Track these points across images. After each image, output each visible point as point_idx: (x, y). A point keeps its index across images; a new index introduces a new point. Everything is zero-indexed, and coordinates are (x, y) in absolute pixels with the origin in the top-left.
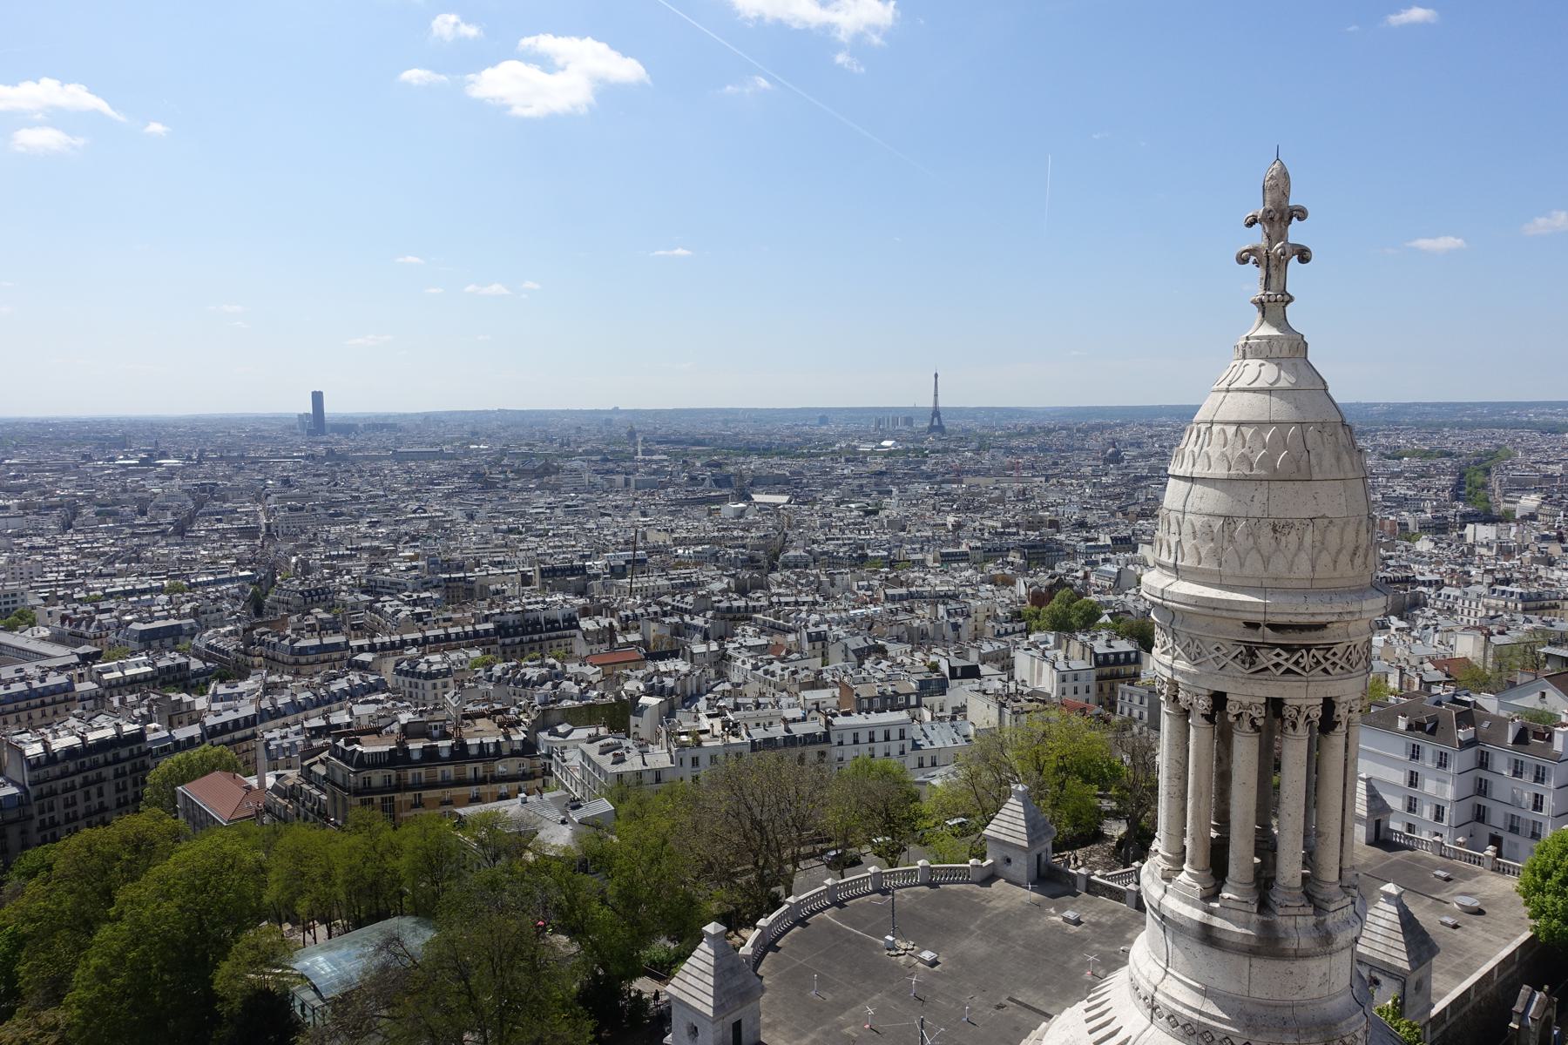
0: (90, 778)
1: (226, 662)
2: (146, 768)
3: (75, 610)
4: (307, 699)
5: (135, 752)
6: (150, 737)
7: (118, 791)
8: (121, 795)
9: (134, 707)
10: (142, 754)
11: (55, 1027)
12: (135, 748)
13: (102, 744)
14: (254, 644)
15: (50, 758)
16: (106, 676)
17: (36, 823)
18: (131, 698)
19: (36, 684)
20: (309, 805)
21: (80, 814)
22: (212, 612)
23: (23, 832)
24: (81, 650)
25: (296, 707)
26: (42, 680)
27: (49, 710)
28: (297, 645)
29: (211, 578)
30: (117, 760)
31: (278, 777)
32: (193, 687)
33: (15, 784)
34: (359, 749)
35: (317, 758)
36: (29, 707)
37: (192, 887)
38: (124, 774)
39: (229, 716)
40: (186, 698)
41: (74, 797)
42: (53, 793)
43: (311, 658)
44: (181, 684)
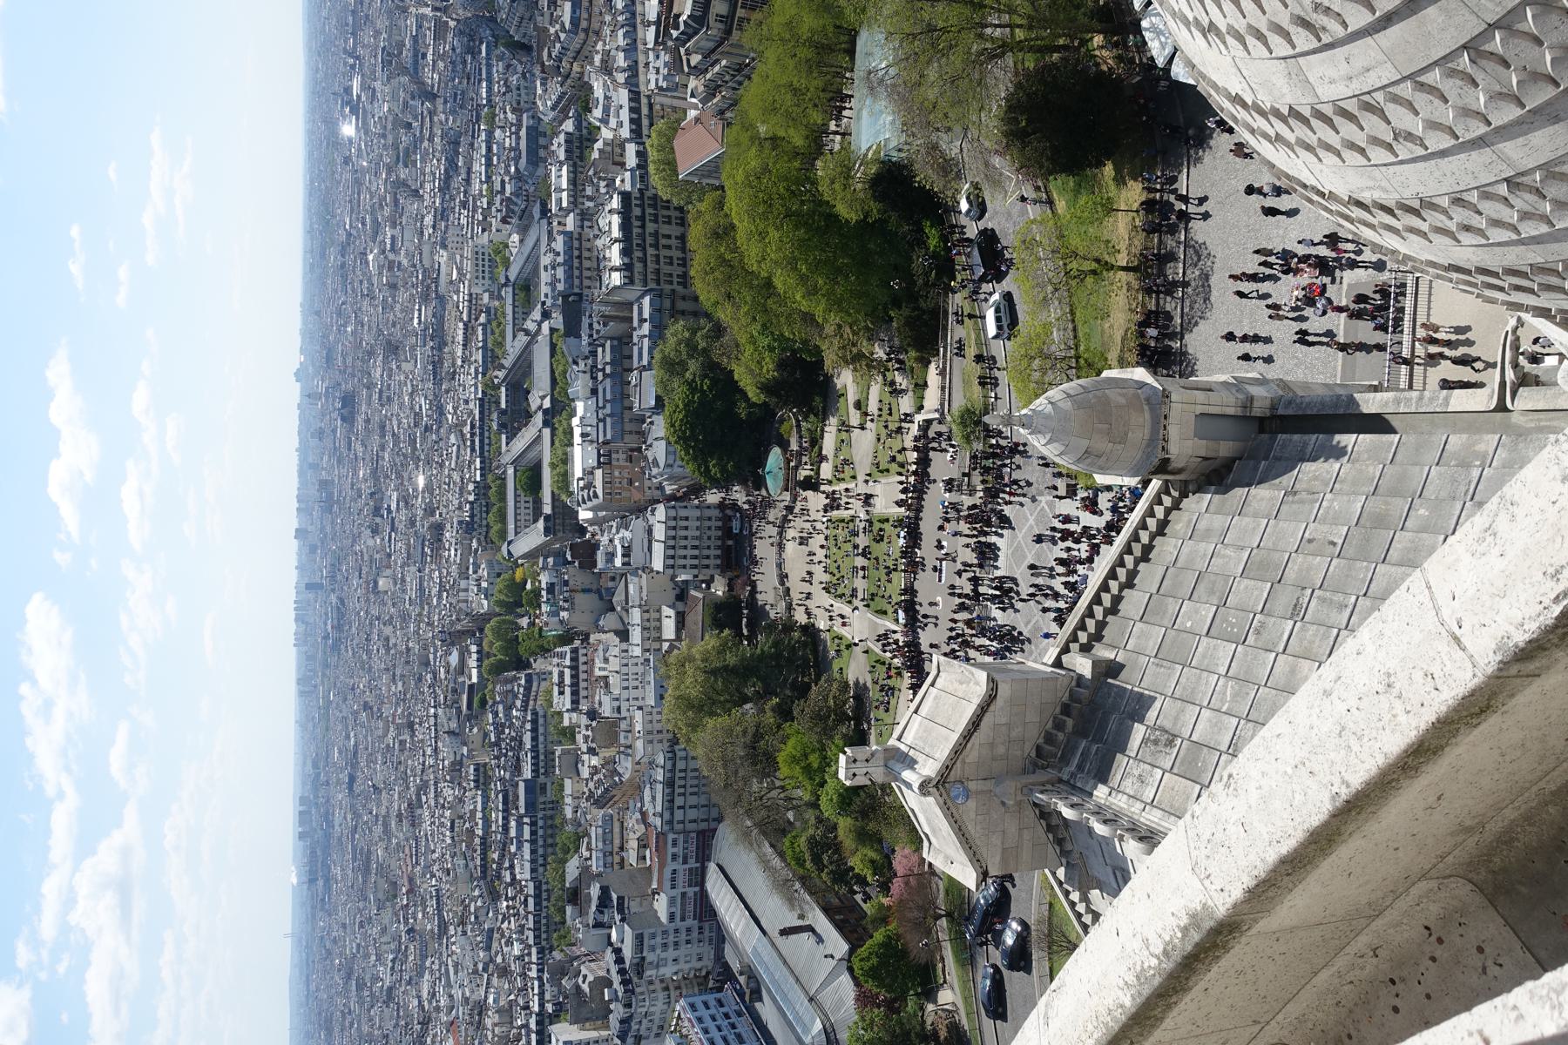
1: (572, 96)
2: (655, 197)
3: (498, 211)
4: (625, 36)
6: (628, 187)
7: (669, 223)
8: (674, 221)
9: (598, 190)
11: (840, 327)
12: (634, 202)
13: (625, 226)
14: (559, 67)
15: (627, 268)
16: (565, 204)
17: (680, 289)
18: (589, 191)
19: (560, 259)
20: (727, 78)
21: (681, 255)
22: (519, 95)
23: (684, 298)
24: (537, 215)
25: (631, 49)
26: (558, 254)
27: (586, 254)
28: (567, 25)
29: (484, 84)
30: (642, 218)
31: (693, 95)
32: (590, 133)
33: (642, 296)
34: (684, 17)
35: (684, 58)
36: (580, 268)
37: (764, 216)
38: (656, 216)
39: (625, 115)
40: (599, 145)
42: (657, 272)
43: (585, 15)
44: (585, 144)
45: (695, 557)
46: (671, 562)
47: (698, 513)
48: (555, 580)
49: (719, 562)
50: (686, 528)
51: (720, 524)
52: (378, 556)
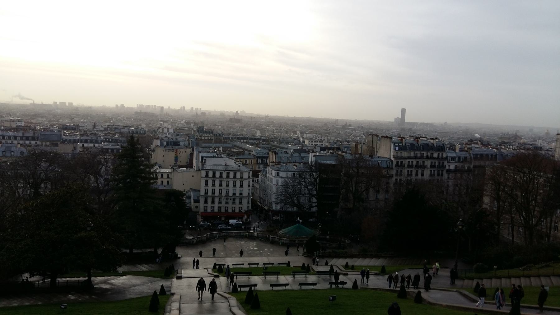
0: (420, 164)
5: (440, 156)
7: (431, 175)
10: (443, 158)
12: (441, 153)
30: (432, 158)
38: (434, 166)
41: (411, 171)
45: (213, 192)
46: (211, 175)
47: (245, 194)
48: (182, 144)
49: (209, 210)
50: (235, 186)
51: (237, 210)
52: (177, 124)
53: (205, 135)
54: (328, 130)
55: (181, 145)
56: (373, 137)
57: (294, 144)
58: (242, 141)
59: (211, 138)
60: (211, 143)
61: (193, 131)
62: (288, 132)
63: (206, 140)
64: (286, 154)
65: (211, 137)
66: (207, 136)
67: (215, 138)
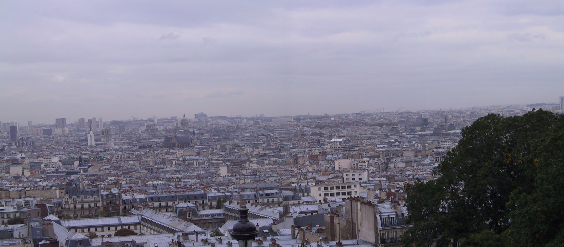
48: (16, 235)
52: (42, 166)
53: (82, 198)
54: (397, 143)
55: (15, 236)
56: (351, 203)
57: (281, 199)
58: (163, 204)
59: (96, 205)
60: (97, 217)
61: (58, 191)
62: (300, 160)
63: (86, 209)
64: (205, 244)
65: (96, 202)
66: (87, 200)
67: (105, 203)
